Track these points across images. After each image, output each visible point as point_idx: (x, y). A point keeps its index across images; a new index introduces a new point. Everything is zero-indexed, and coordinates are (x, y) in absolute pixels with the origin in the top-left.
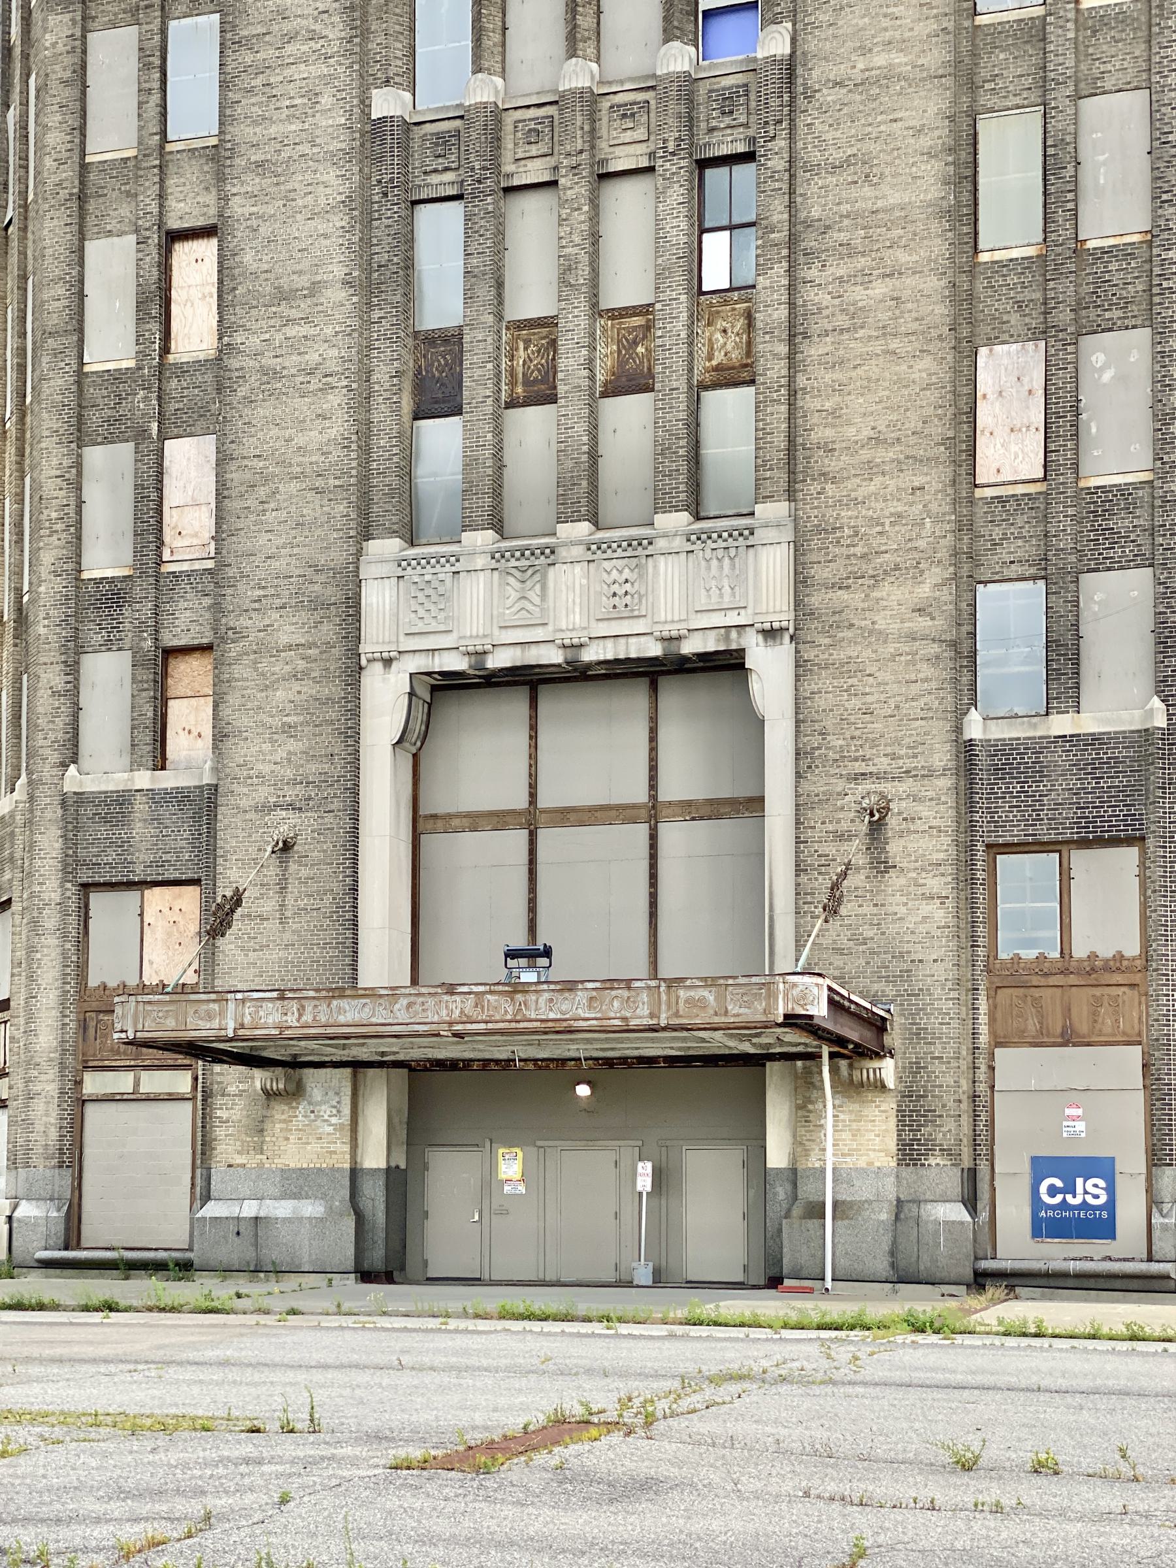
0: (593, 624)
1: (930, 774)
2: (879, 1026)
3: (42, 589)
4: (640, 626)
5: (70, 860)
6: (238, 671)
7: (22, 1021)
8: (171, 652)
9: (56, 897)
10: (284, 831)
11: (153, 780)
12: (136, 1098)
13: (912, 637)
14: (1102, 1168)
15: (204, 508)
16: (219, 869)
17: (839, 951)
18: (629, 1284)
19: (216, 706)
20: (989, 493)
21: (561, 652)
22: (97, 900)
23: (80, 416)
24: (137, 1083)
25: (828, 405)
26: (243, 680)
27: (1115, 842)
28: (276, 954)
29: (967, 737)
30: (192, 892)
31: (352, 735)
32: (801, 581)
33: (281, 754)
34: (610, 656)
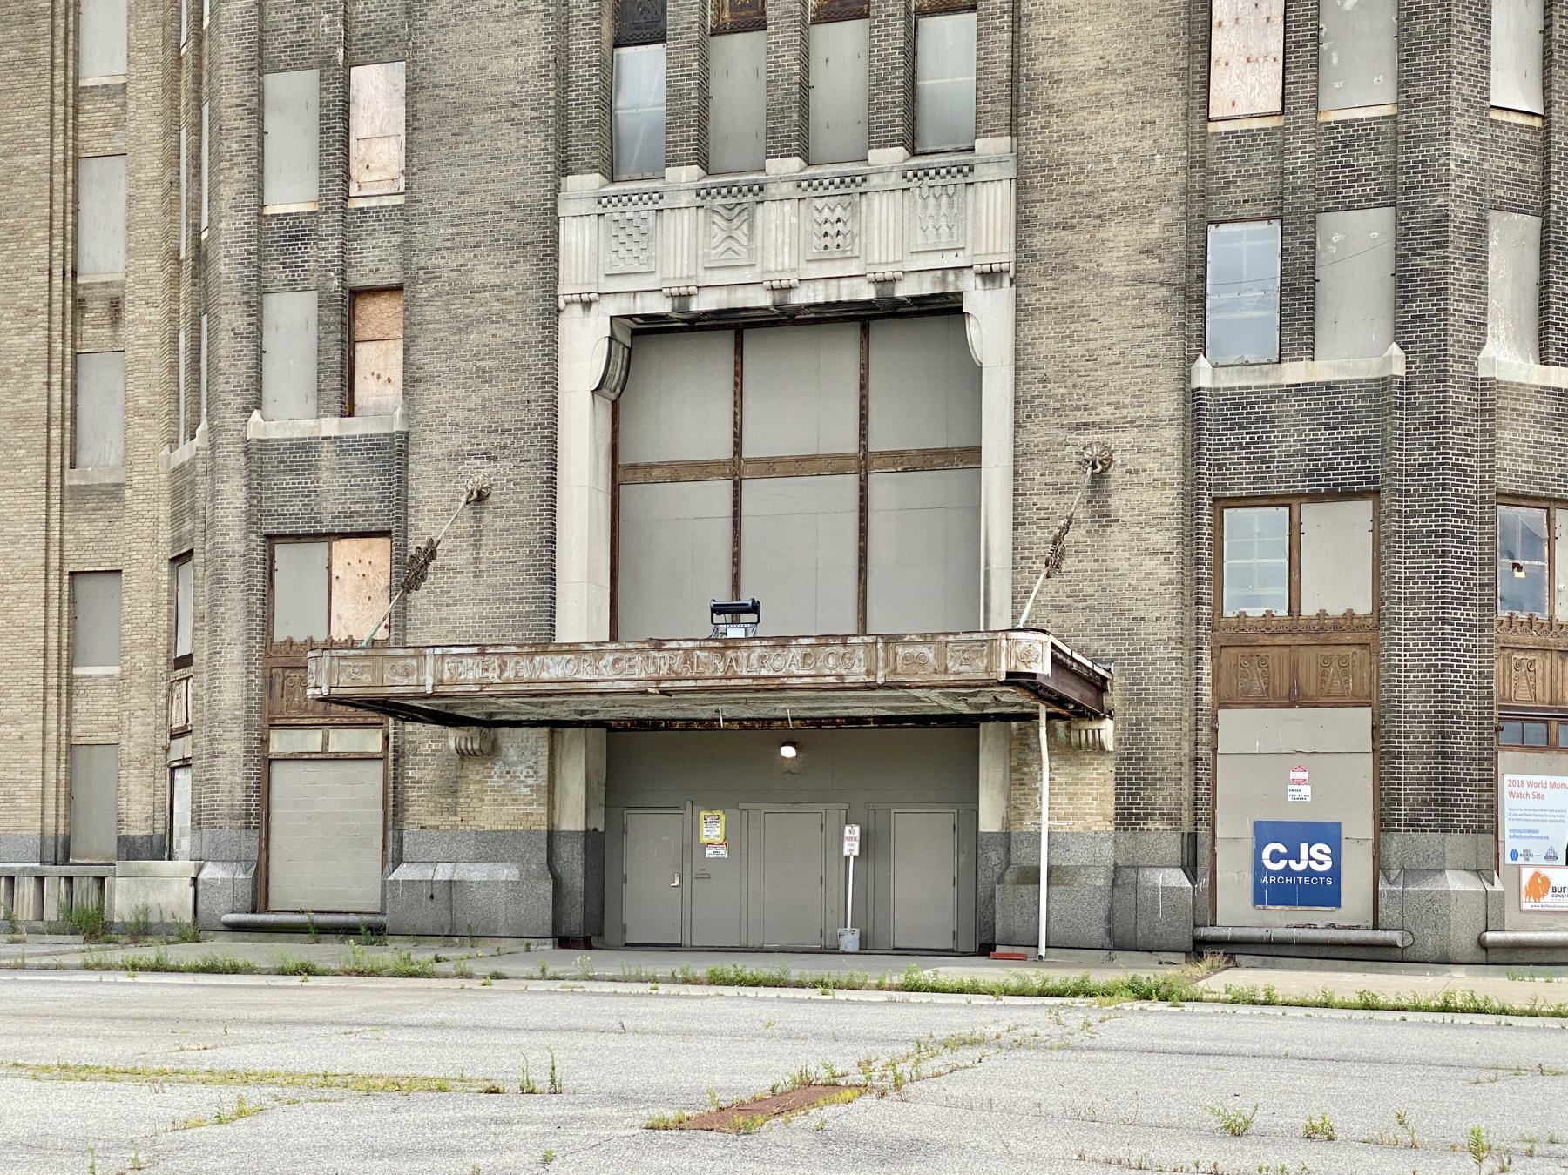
0: (803, 265)
1: (1155, 424)
2: (1099, 685)
3: (223, 225)
4: (853, 268)
5: (255, 510)
6: (429, 312)
7: (205, 676)
8: (357, 293)
9: (240, 548)
10: (478, 480)
11: (340, 426)
13: (1139, 280)
14: (1328, 833)
15: (393, 140)
17: (1058, 608)
18: (835, 951)
19: (406, 350)
20: (1222, 127)
21: (769, 295)
22: (282, 552)
23: (261, 41)
24: (326, 742)
25: (1054, 33)
27: (1348, 495)
28: (470, 610)
29: (1195, 385)
30: (382, 544)
31: (550, 381)
32: (1023, 221)
33: (475, 400)
34: (821, 299)
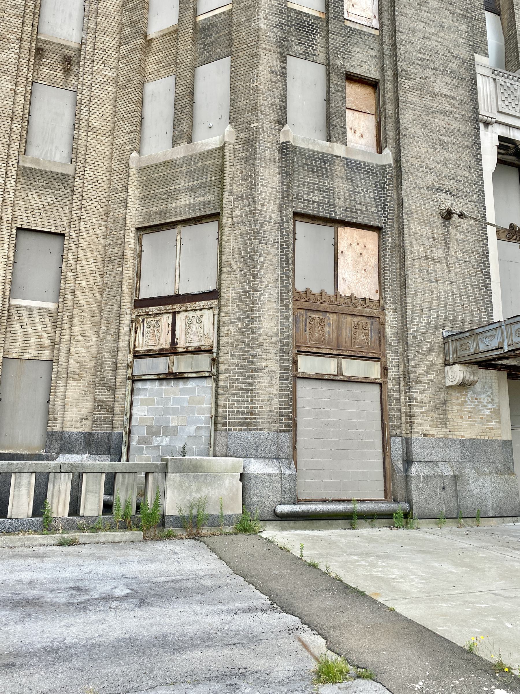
9: (276, 217)
16: (406, 222)
24: (340, 368)
31: (478, 158)
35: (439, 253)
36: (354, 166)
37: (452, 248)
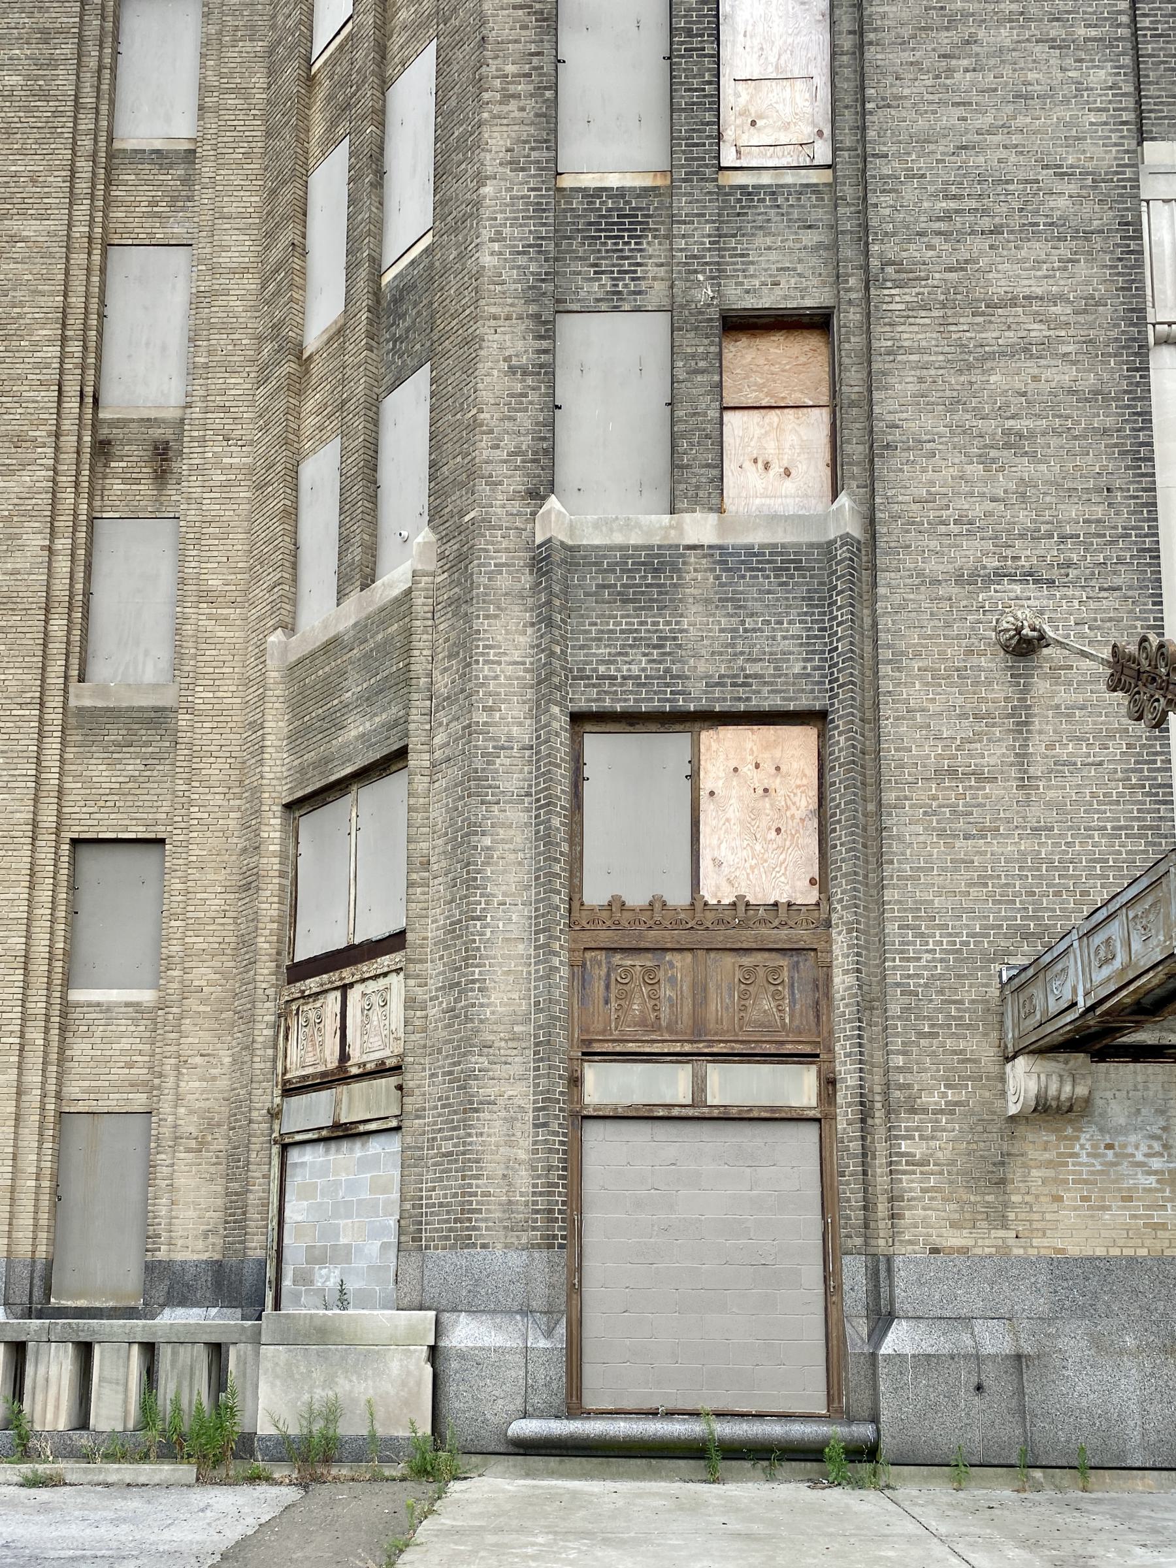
6: (908, 335)
12: (699, 1116)
16: (886, 685)
22: (599, 748)
26: (921, 351)
33: (1003, 483)
35: (995, 753)
36: (743, 562)
37: (1040, 732)
